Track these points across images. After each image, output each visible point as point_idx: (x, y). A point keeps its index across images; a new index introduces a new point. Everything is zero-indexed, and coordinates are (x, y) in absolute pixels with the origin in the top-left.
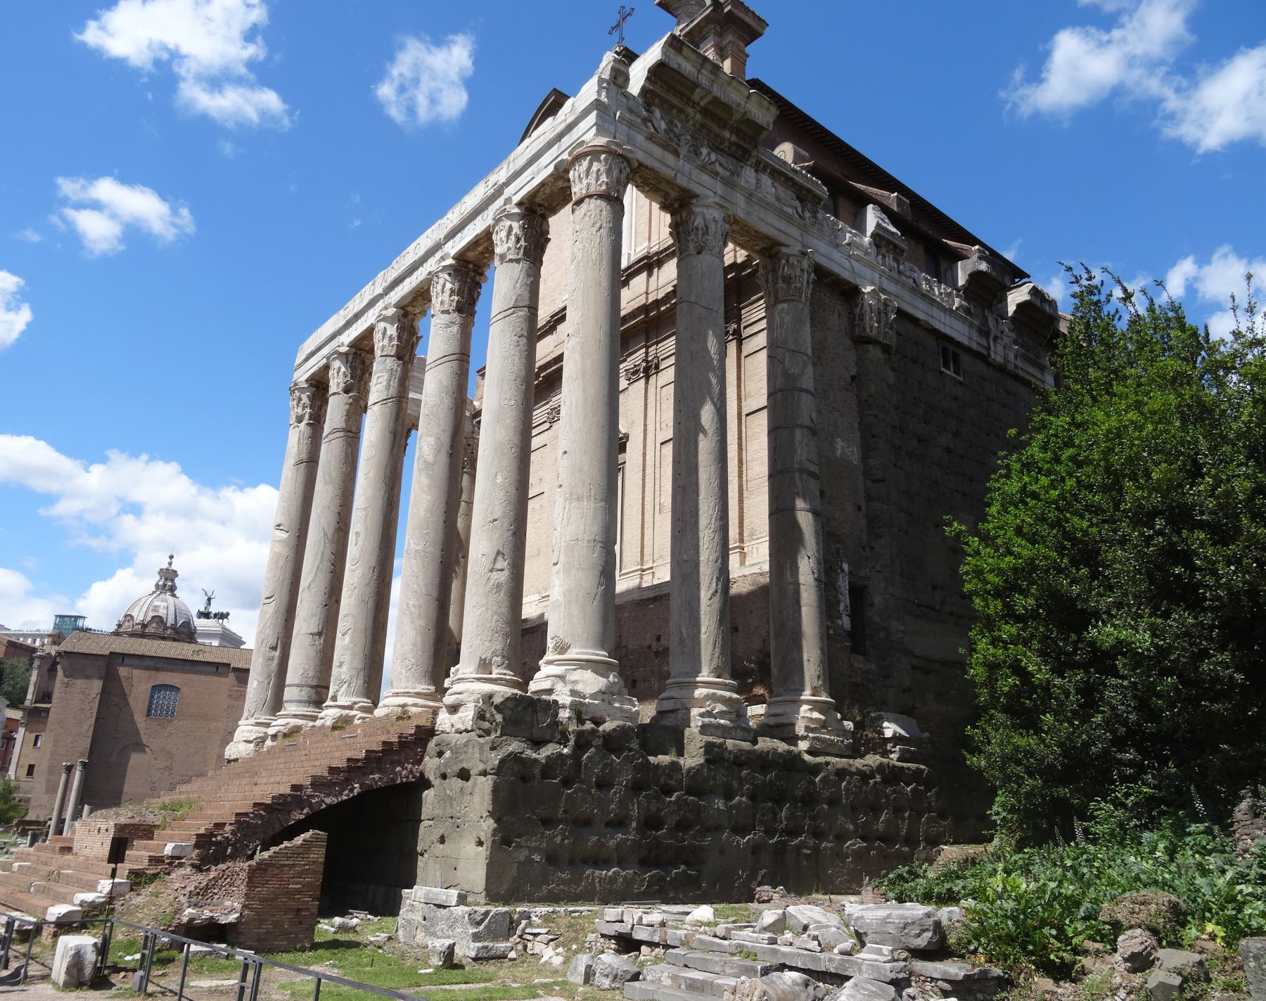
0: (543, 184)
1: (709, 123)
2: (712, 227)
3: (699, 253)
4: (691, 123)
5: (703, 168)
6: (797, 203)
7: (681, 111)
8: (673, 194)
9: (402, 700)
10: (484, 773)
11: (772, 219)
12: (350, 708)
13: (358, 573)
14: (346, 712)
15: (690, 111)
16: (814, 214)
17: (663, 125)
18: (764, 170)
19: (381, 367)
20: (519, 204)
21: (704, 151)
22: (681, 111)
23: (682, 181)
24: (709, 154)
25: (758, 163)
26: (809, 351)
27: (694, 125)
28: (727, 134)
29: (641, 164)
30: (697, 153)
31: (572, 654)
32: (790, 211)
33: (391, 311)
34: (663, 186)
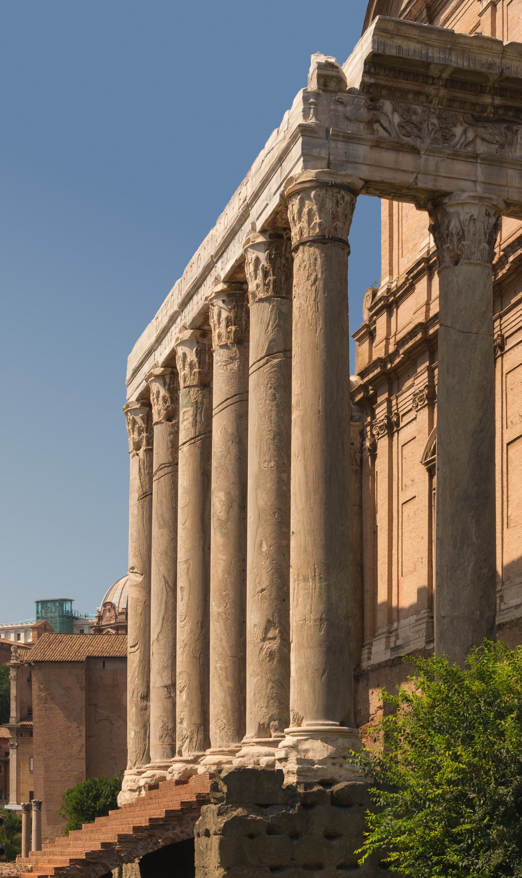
1: (460, 95)
3: (456, 263)
4: (435, 101)
7: (418, 93)
13: (187, 628)
19: (186, 400)
21: (458, 131)
22: (418, 93)
24: (465, 132)
27: (440, 102)
28: (487, 99)
30: (447, 138)
34: (405, 191)
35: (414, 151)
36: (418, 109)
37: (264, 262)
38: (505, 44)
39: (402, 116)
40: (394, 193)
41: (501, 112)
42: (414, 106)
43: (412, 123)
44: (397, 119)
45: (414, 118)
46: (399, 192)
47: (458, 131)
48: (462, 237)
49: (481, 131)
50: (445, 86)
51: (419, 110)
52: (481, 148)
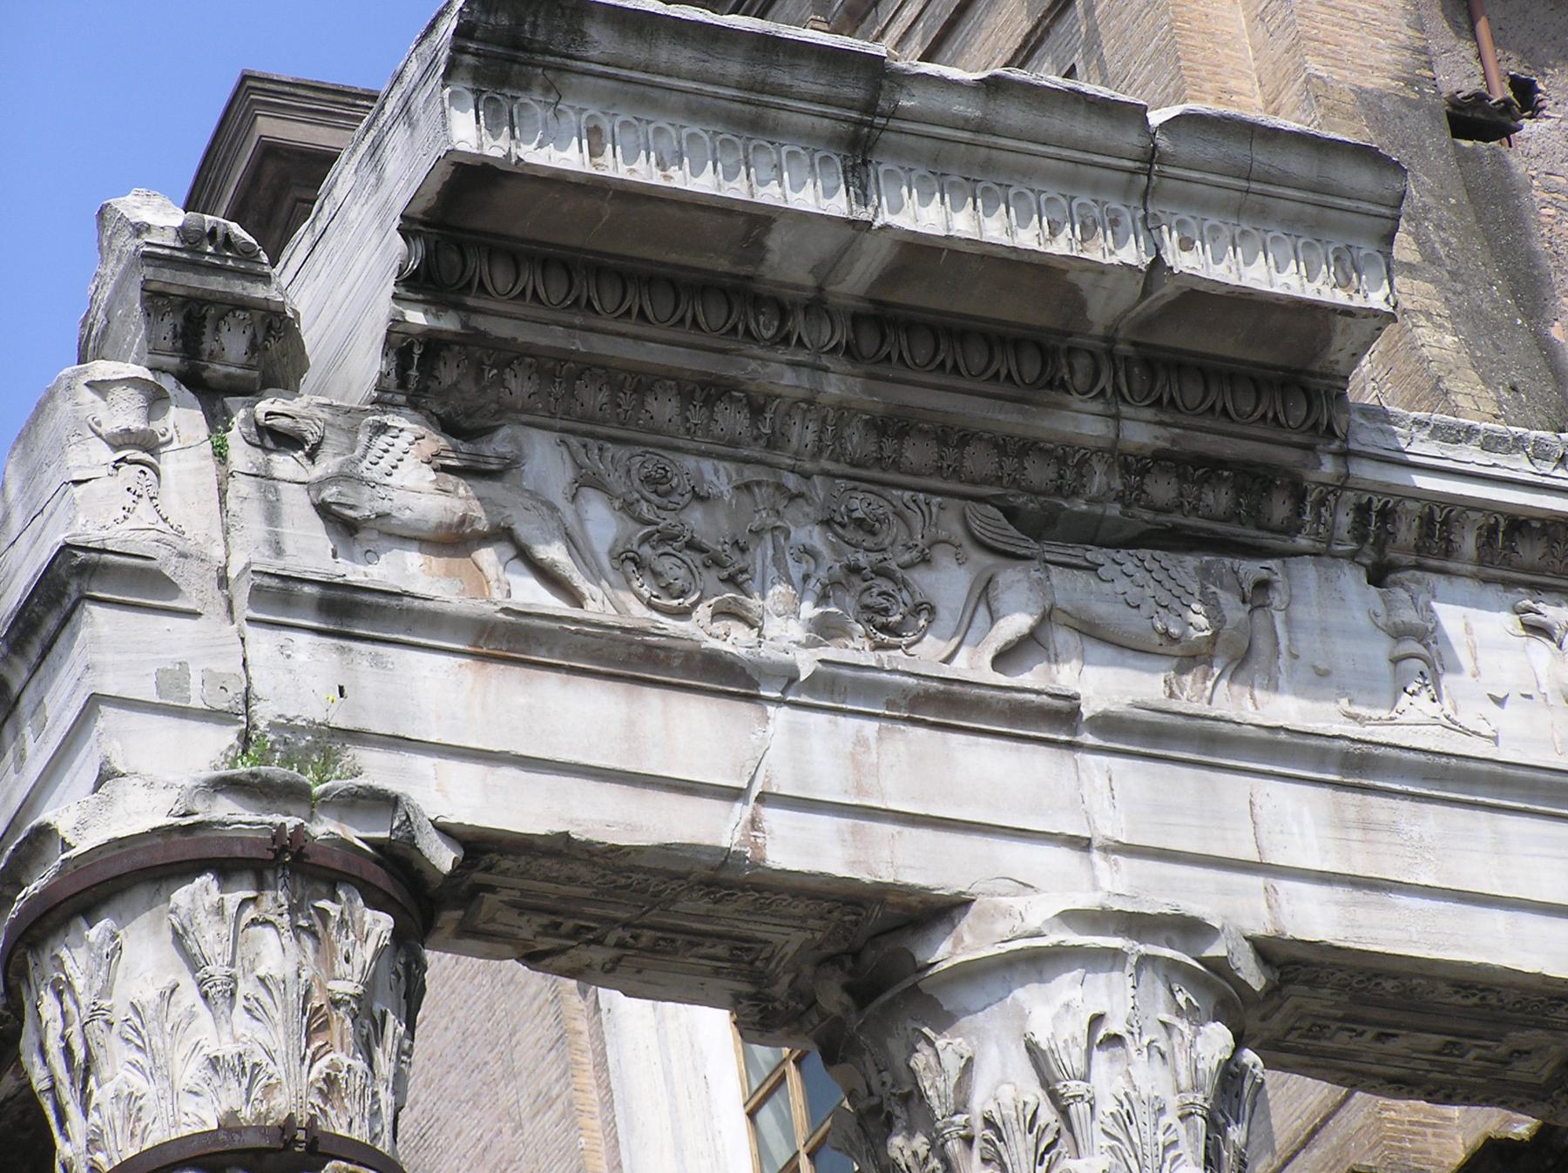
4: (803, 434)
5: (945, 707)
7: (712, 391)
8: (787, 940)
15: (780, 375)
23: (798, 847)
28: (1083, 423)
29: (477, 846)
36: (709, 476)
38: (1156, 118)
39: (627, 508)
40: (626, 925)
41: (1162, 489)
42: (690, 462)
43: (692, 545)
44: (602, 523)
45: (696, 520)
46: (654, 917)
47: (948, 583)
49: (1071, 588)
50: (850, 352)
51: (718, 477)
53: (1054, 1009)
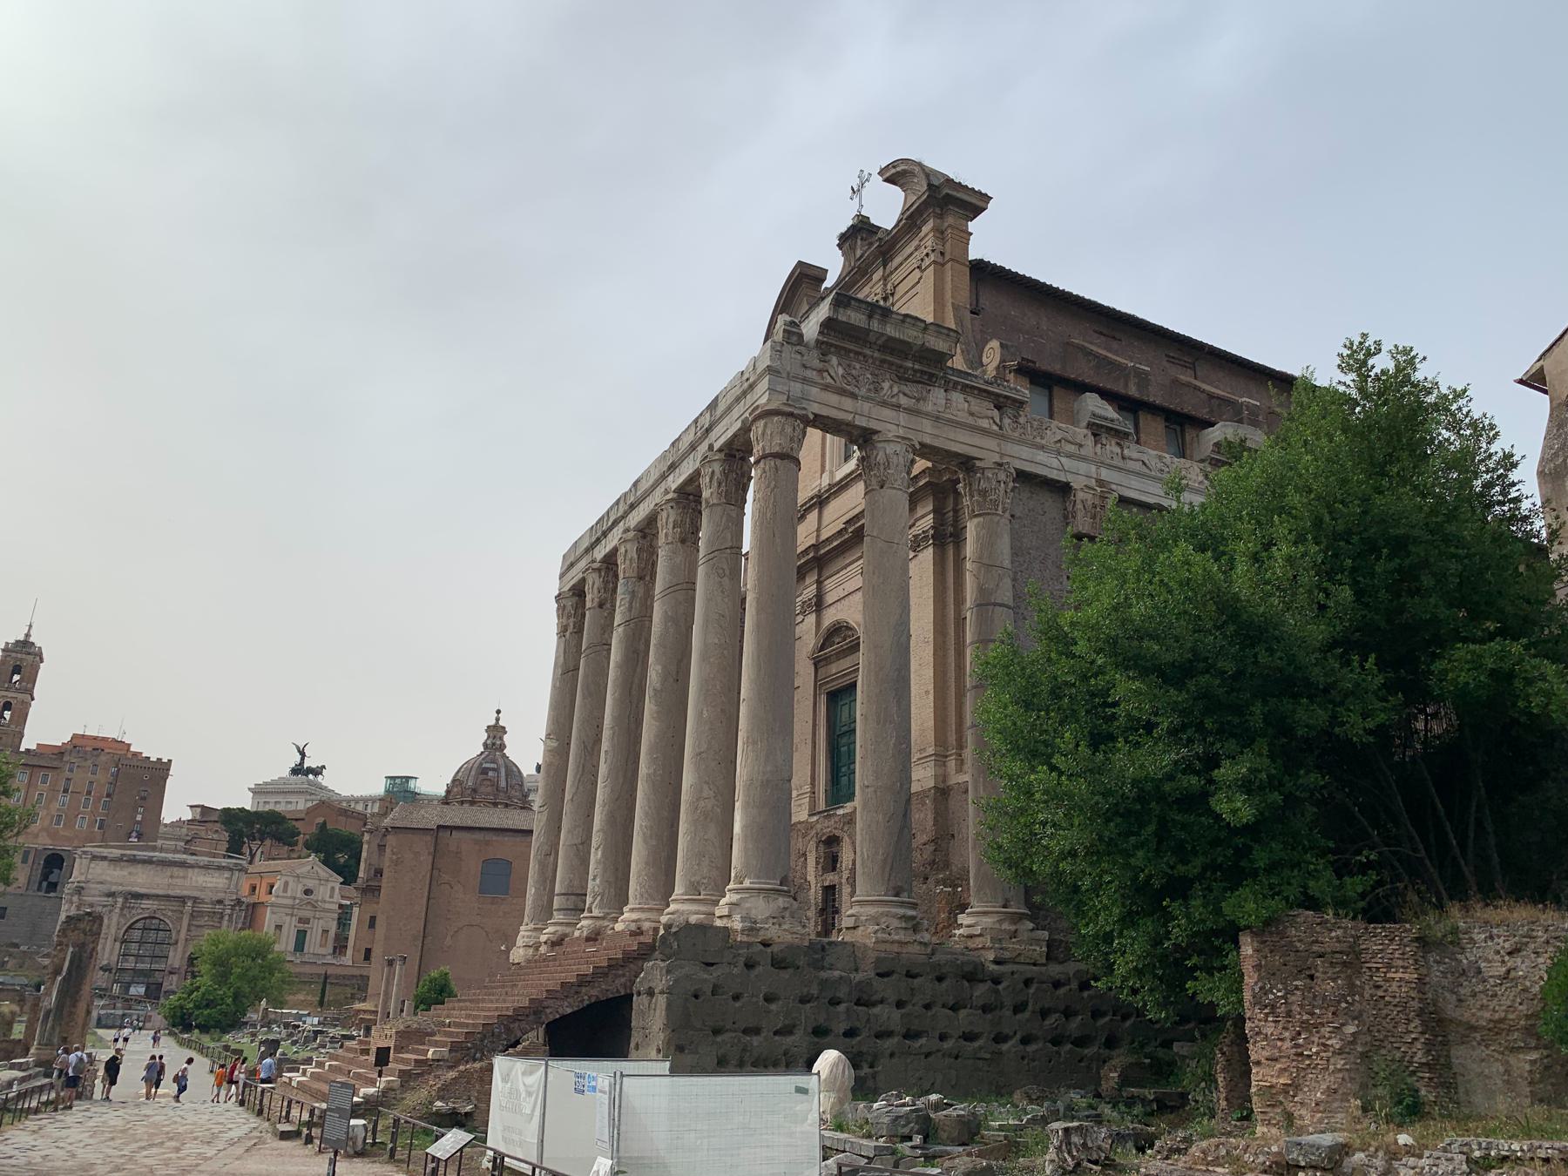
0: (735, 435)
2: (894, 460)
5: (884, 404)
6: (996, 413)
8: (856, 433)
9: (635, 916)
10: (662, 992)
11: (963, 436)
12: (603, 918)
14: (599, 923)
15: (868, 352)
16: (1015, 419)
17: (841, 371)
18: (955, 388)
20: (720, 450)
21: (886, 385)
22: (857, 353)
23: (861, 422)
25: (947, 382)
26: (1007, 563)
29: (816, 415)
31: (747, 883)
32: (985, 423)
33: (631, 534)
35: (854, 396)
37: (717, 475)
47: (886, 385)
48: (888, 466)
49: (904, 388)
52: (903, 401)
53: (890, 448)
